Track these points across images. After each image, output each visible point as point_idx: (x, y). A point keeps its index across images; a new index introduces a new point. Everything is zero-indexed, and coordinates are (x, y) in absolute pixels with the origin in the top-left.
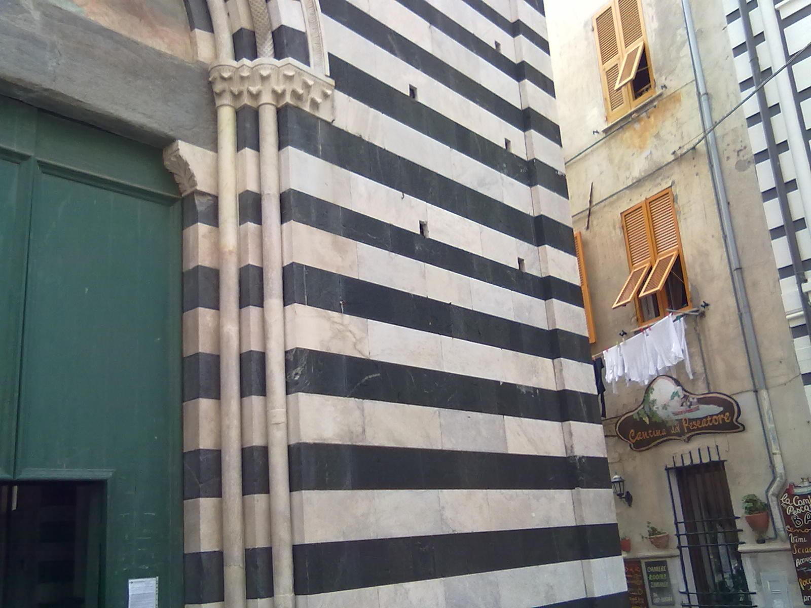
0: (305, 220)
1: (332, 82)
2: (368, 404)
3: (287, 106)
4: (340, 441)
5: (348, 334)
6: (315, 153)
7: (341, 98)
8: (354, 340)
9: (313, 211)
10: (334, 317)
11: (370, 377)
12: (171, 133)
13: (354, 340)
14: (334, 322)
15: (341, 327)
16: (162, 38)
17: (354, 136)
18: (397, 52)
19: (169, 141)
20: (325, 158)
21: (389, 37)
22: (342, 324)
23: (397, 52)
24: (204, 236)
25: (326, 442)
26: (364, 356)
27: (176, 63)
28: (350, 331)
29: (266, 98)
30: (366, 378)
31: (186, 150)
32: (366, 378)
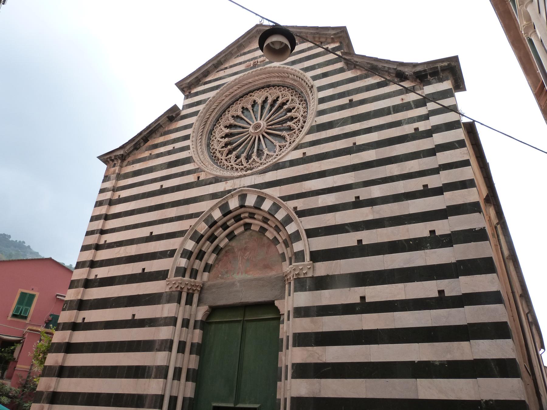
0: (298, 316)
1: (311, 262)
2: (323, 381)
3: (295, 279)
4: (308, 395)
5: (316, 354)
6: (306, 290)
7: (318, 265)
8: (318, 356)
9: (303, 312)
10: (309, 349)
11: (325, 369)
12: (273, 299)
13: (318, 356)
14: (309, 351)
15: (312, 352)
16: (274, 270)
17: (325, 276)
18: (350, 230)
19: (274, 301)
20: (310, 290)
21: (346, 227)
22: (313, 351)
23: (350, 230)
24: (282, 328)
25: (301, 396)
26: (322, 361)
27: (275, 277)
28: (317, 353)
29: (292, 279)
30: (323, 370)
31: (277, 303)
32: (323, 370)
